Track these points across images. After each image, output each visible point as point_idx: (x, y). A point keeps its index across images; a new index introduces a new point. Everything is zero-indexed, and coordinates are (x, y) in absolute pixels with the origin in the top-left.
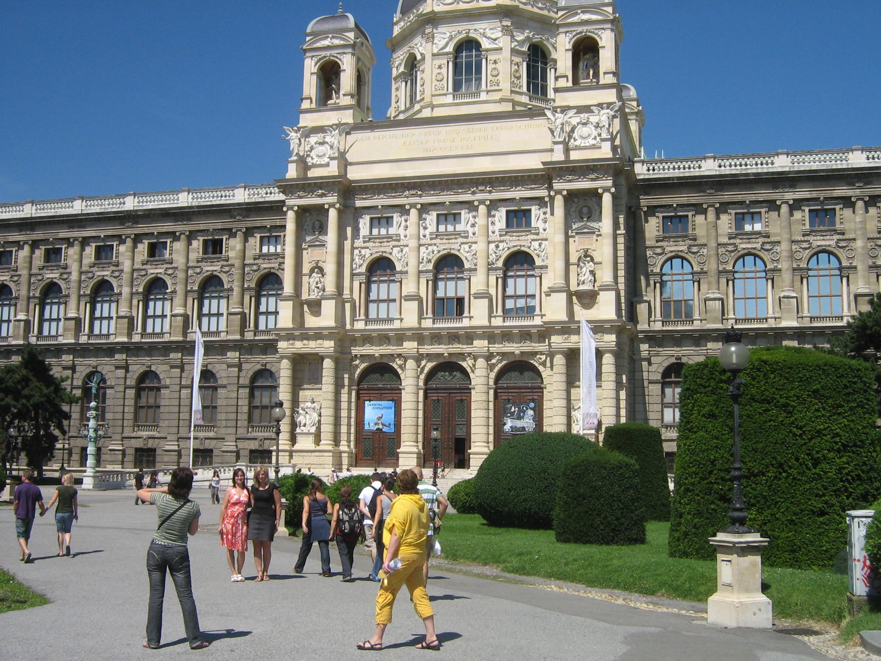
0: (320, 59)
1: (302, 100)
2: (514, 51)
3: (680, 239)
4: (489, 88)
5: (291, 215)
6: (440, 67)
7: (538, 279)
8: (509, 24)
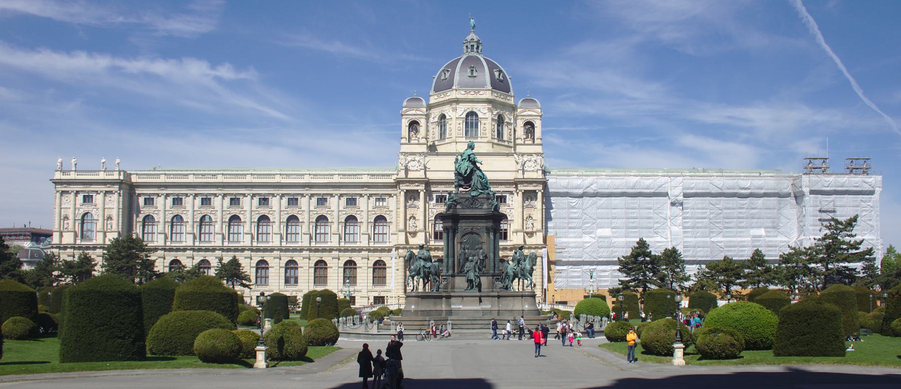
0: (409, 120)
1: (402, 138)
2: (493, 120)
4: (482, 136)
7: (509, 225)
8: (491, 107)
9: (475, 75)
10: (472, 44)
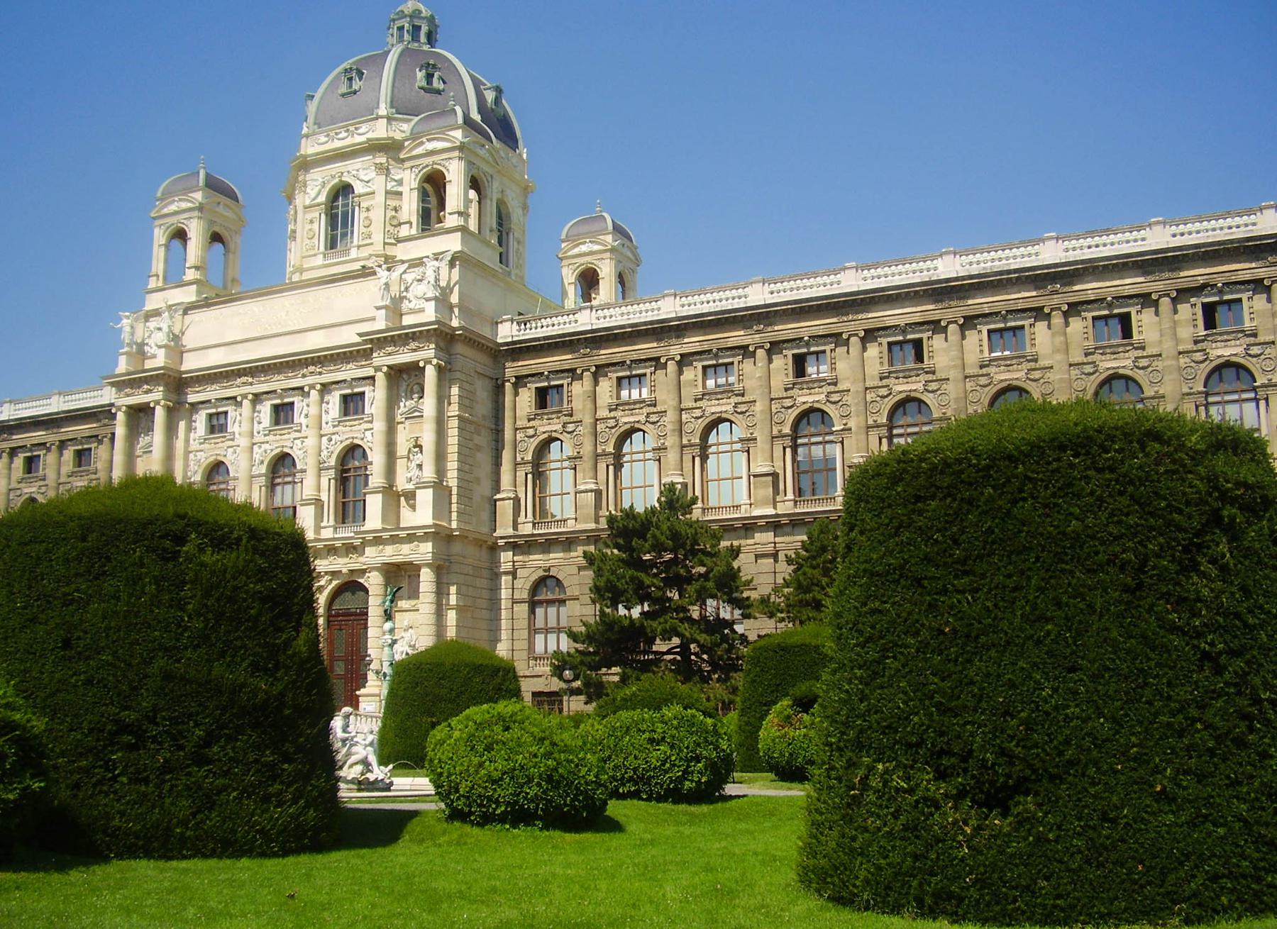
3: (553, 416)
5: (121, 417)
6: (311, 222)
8: (383, 160)
9: (355, 87)
10: (399, 23)
